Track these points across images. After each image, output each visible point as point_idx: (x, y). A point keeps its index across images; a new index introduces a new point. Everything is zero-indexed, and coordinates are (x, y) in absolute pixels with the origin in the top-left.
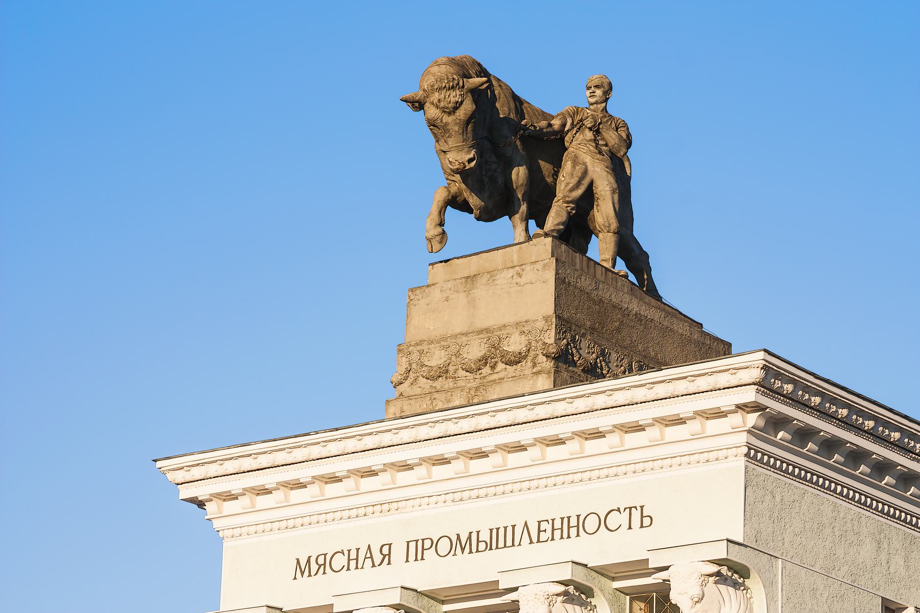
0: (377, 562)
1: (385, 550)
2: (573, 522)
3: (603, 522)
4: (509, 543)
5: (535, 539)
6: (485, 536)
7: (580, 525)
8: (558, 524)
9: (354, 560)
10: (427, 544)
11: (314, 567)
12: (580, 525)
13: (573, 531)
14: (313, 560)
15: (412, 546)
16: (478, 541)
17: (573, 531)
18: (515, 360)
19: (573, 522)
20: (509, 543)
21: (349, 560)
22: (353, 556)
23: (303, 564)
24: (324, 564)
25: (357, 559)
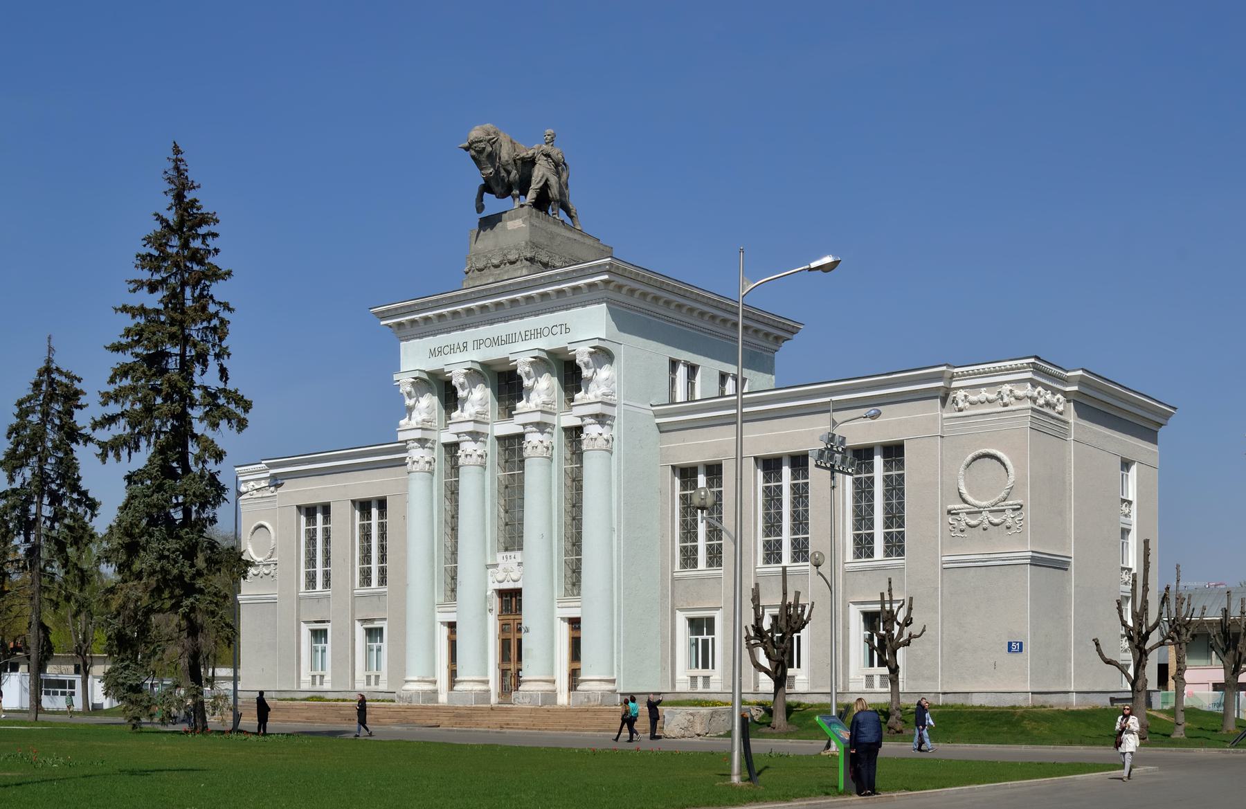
0: (462, 349)
1: (465, 345)
2: (539, 331)
3: (550, 331)
6: (504, 338)
9: (453, 349)
10: (481, 342)
11: (437, 353)
13: (539, 335)
17: (539, 335)
18: (512, 263)
19: (539, 331)
22: (452, 347)
23: (432, 351)
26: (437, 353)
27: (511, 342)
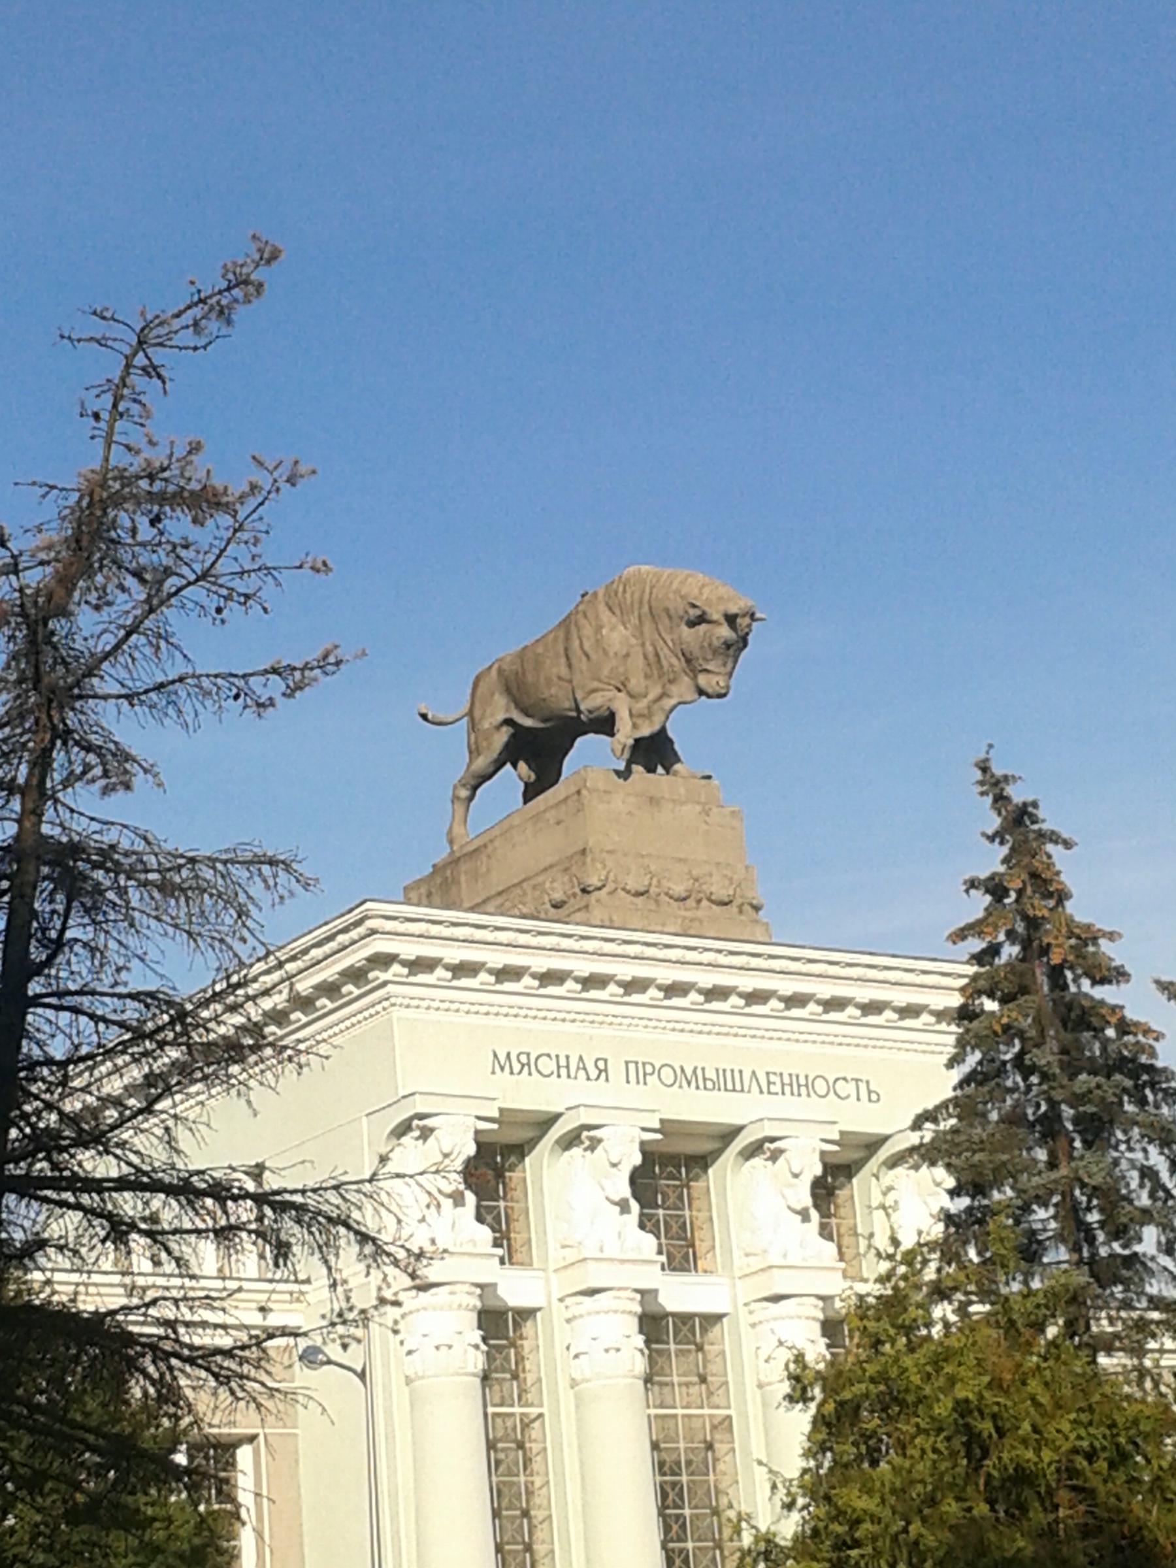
3: (832, 1088)
4: (738, 1087)
5: (765, 1089)
7: (809, 1086)
8: (786, 1080)
11: (517, 1067)
12: (809, 1086)
14: (513, 1057)
15: (632, 1067)
16: (705, 1079)
19: (802, 1081)
20: (738, 1087)
21: (559, 1067)
22: (563, 1062)
23: (502, 1058)
24: (528, 1064)
25: (568, 1067)
26: (517, 1067)
27: (730, 1086)
